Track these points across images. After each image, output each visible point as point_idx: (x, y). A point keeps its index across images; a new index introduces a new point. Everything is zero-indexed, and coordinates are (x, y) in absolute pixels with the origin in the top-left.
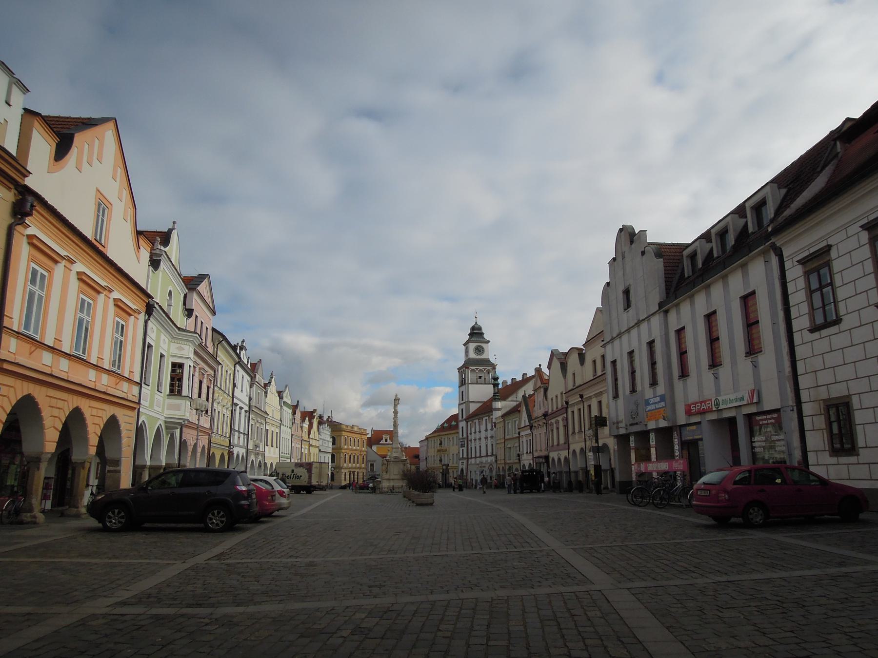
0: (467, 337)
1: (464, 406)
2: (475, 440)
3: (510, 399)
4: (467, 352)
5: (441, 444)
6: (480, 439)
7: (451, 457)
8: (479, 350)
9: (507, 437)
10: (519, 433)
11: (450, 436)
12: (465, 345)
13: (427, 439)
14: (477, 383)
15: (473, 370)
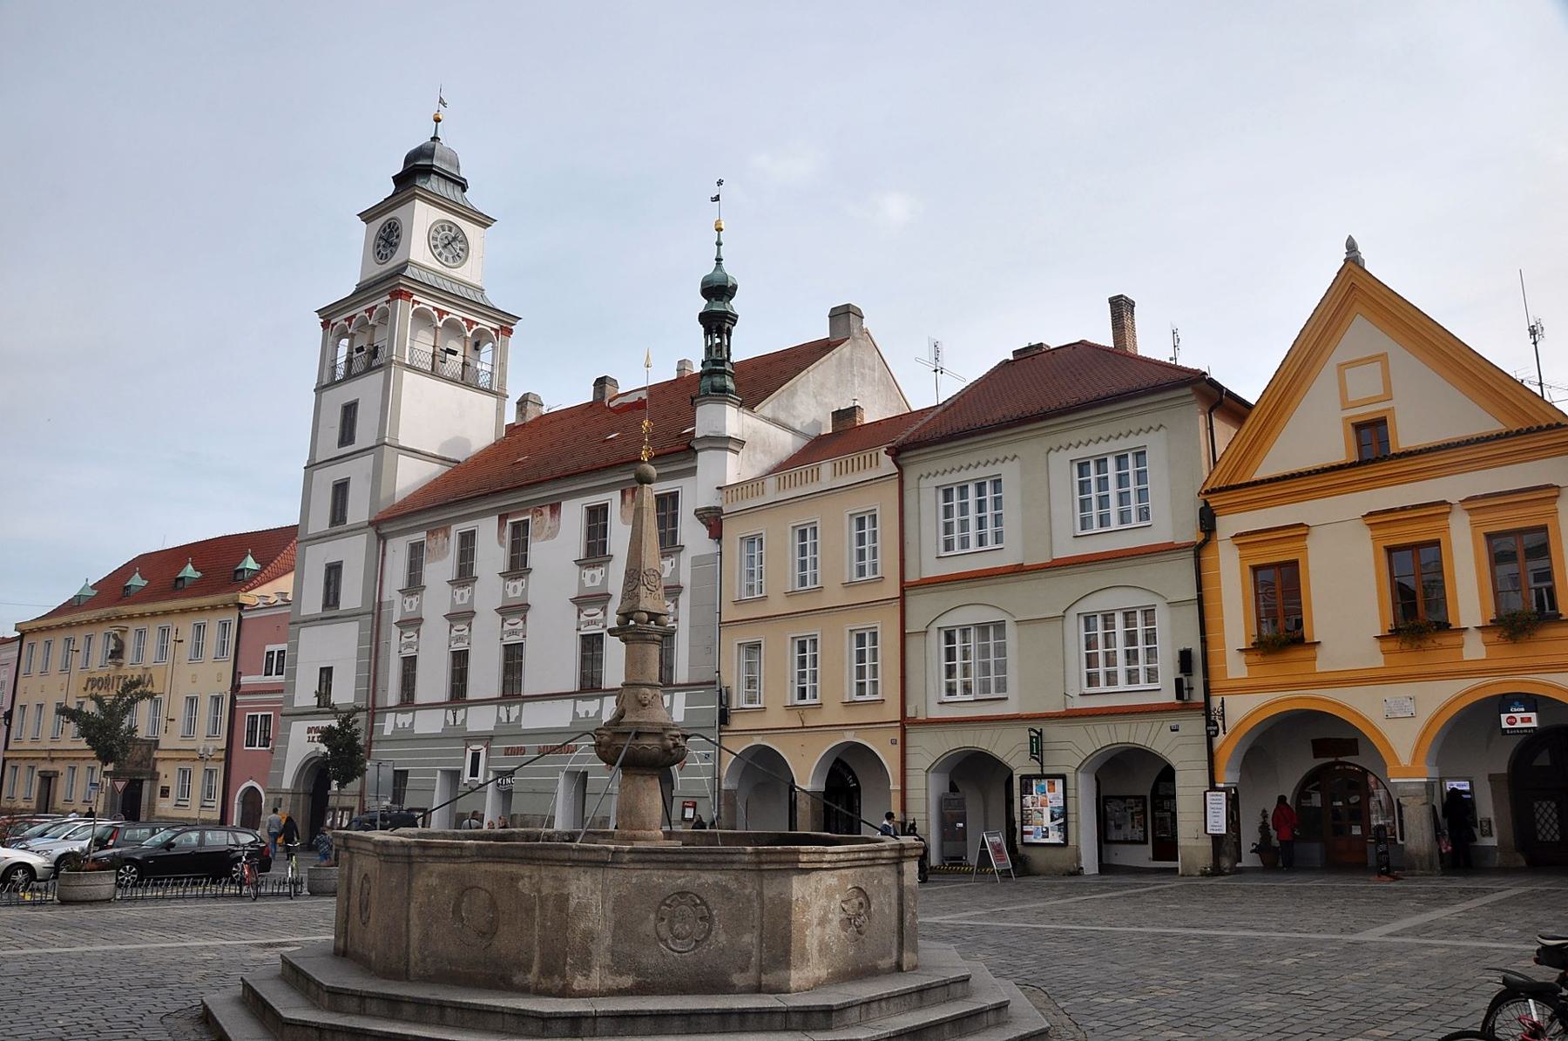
0: (391, 188)
1: (357, 472)
2: (461, 616)
3: (767, 407)
4: (389, 239)
5: (117, 653)
6: (515, 610)
7: (179, 710)
8: (451, 244)
9: (932, 570)
10: (1208, 521)
11: (185, 627)
12: (367, 216)
13: (26, 632)
14: (434, 373)
15: (422, 317)
